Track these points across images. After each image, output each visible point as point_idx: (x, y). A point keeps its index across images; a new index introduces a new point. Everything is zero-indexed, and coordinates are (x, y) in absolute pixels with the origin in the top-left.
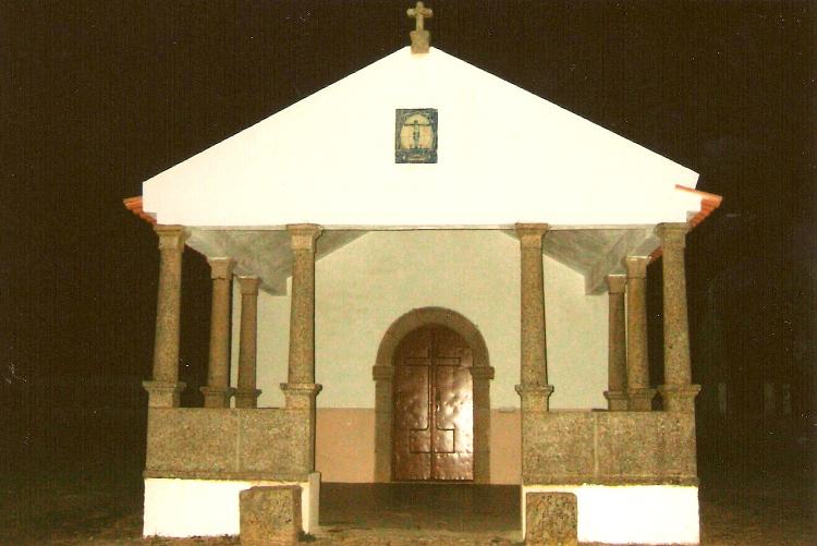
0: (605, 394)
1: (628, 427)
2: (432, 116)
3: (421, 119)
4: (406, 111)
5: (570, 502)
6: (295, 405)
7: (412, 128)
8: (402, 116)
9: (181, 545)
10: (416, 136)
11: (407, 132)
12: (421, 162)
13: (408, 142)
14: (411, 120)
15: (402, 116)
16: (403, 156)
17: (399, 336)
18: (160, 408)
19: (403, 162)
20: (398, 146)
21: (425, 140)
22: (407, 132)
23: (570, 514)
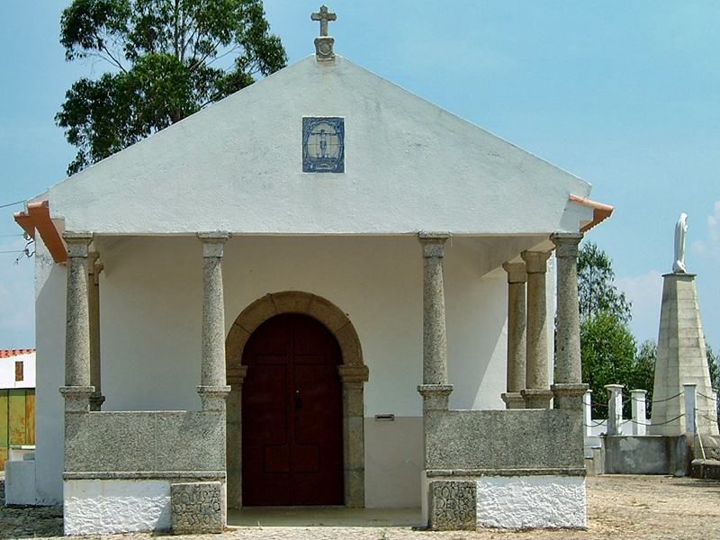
0: (503, 395)
1: (523, 423)
2: (339, 125)
3: (328, 129)
4: (313, 119)
5: (472, 487)
6: (211, 407)
7: (318, 136)
8: (309, 125)
9: (104, 538)
10: (323, 145)
11: (314, 141)
12: (328, 171)
13: (315, 151)
14: (319, 129)
15: (309, 125)
16: (310, 165)
17: (251, 328)
18: (77, 413)
19: (310, 170)
20: (306, 156)
21: (332, 151)
22: (314, 141)
23: (470, 496)
